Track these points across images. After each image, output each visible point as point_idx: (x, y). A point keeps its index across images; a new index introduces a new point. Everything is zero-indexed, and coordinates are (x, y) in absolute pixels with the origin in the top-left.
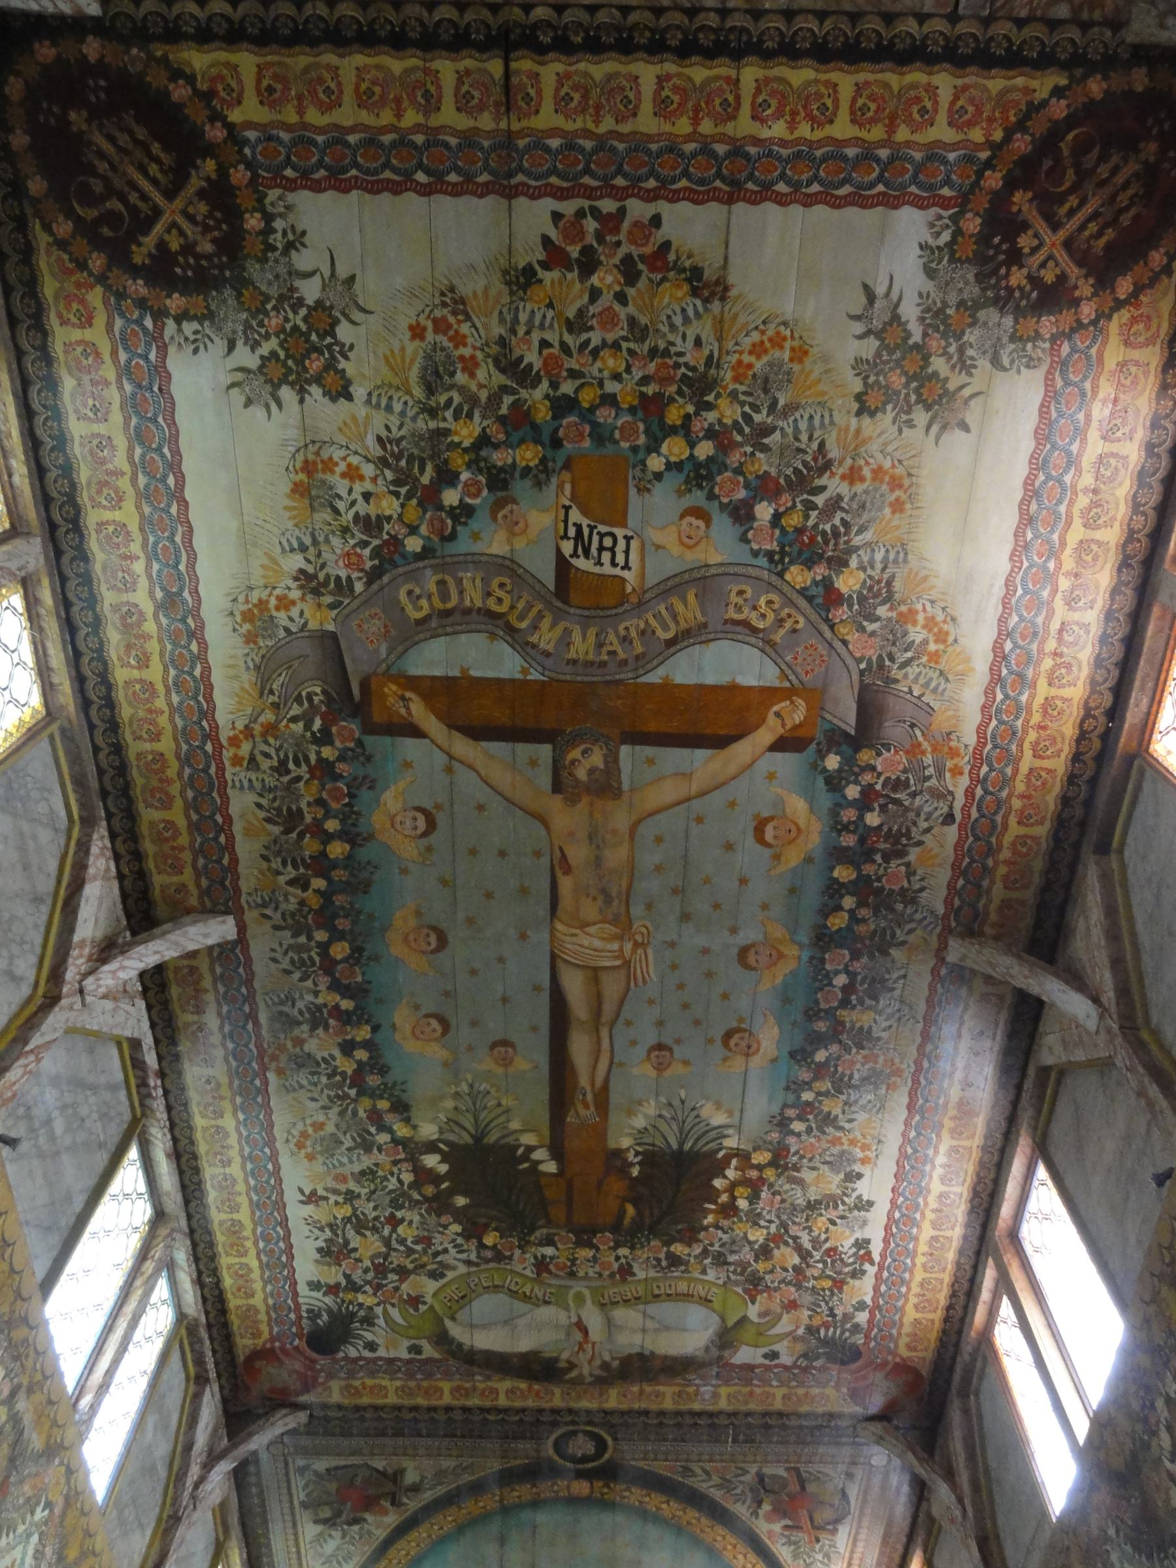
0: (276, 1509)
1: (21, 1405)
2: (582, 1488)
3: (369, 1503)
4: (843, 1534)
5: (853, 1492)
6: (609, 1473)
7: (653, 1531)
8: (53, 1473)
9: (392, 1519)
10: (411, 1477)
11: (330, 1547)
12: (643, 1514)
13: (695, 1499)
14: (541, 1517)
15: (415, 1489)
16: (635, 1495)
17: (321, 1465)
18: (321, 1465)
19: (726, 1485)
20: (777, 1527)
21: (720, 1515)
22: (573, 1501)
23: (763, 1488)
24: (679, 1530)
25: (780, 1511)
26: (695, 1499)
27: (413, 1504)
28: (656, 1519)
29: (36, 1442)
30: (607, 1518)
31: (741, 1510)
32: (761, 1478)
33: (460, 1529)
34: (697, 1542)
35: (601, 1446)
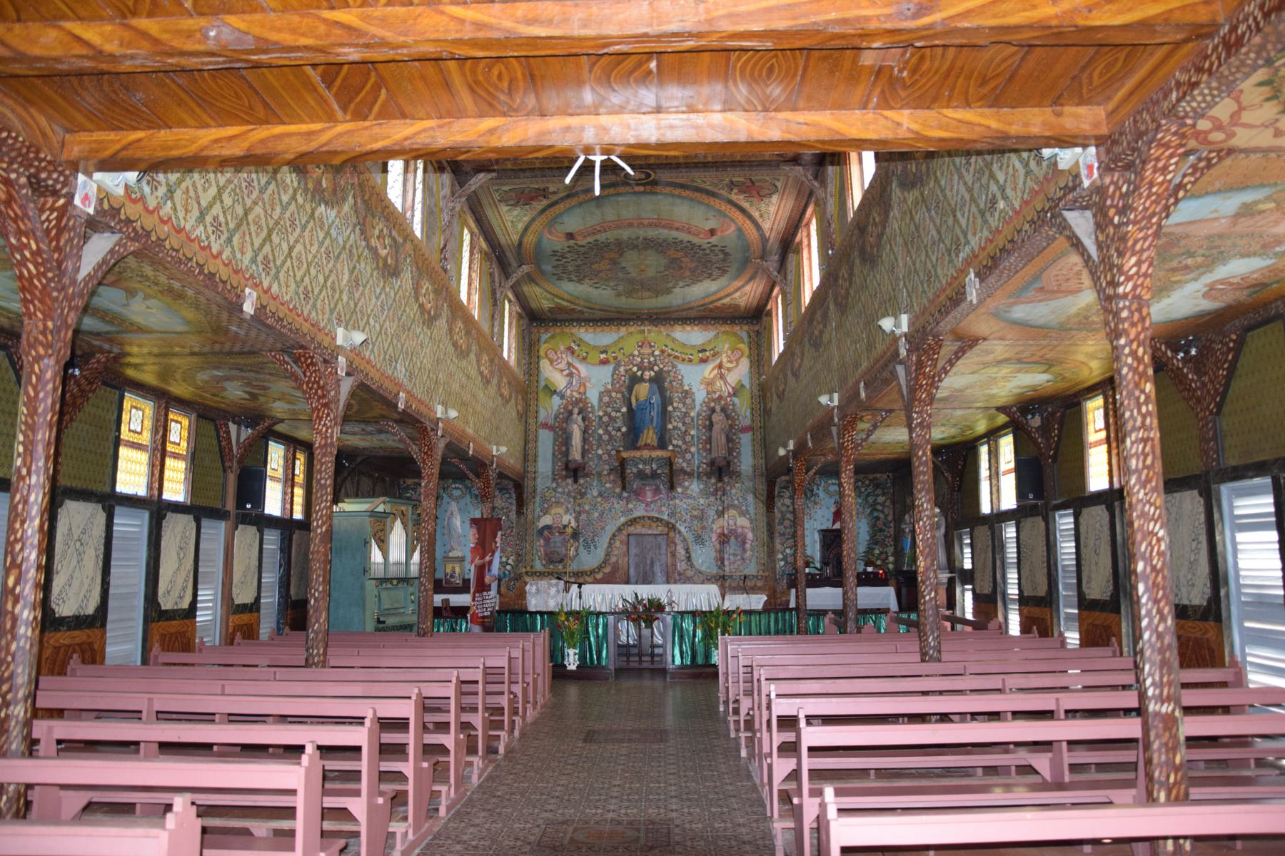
0: (485, 202)
1: (394, 233)
2: (642, 189)
3: (532, 199)
4: (775, 198)
5: (779, 184)
6: (655, 183)
7: (679, 201)
8: (408, 246)
9: (545, 202)
10: (552, 189)
11: (515, 213)
12: (673, 195)
13: (698, 190)
14: (620, 199)
15: (554, 193)
16: (668, 190)
17: (506, 188)
18: (506, 188)
19: (716, 185)
20: (741, 197)
21: (713, 194)
22: (635, 193)
23: (732, 186)
24: (692, 200)
25: (741, 192)
26: (698, 190)
27: (554, 198)
28: (679, 196)
29: (400, 240)
30: (654, 198)
31: (724, 192)
32: (732, 182)
33: (580, 204)
34: (701, 203)
35: (648, 175)
